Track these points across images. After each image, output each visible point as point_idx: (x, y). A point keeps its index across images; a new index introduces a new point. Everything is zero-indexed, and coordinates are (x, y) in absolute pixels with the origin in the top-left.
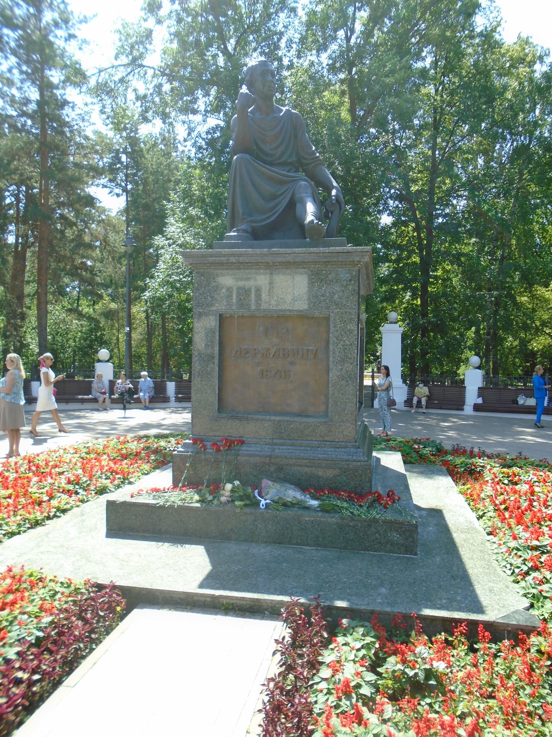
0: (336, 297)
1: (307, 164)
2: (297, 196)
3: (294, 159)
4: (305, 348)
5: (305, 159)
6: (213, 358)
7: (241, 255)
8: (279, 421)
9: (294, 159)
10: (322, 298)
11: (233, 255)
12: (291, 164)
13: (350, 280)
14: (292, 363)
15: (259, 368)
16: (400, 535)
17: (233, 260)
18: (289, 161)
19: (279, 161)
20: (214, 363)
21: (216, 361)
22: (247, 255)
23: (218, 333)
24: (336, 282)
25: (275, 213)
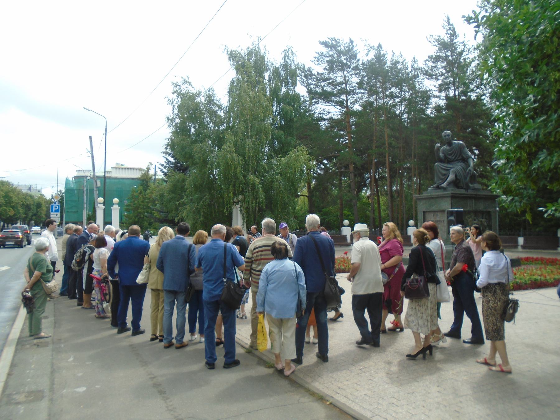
9: (460, 158)
12: (460, 159)
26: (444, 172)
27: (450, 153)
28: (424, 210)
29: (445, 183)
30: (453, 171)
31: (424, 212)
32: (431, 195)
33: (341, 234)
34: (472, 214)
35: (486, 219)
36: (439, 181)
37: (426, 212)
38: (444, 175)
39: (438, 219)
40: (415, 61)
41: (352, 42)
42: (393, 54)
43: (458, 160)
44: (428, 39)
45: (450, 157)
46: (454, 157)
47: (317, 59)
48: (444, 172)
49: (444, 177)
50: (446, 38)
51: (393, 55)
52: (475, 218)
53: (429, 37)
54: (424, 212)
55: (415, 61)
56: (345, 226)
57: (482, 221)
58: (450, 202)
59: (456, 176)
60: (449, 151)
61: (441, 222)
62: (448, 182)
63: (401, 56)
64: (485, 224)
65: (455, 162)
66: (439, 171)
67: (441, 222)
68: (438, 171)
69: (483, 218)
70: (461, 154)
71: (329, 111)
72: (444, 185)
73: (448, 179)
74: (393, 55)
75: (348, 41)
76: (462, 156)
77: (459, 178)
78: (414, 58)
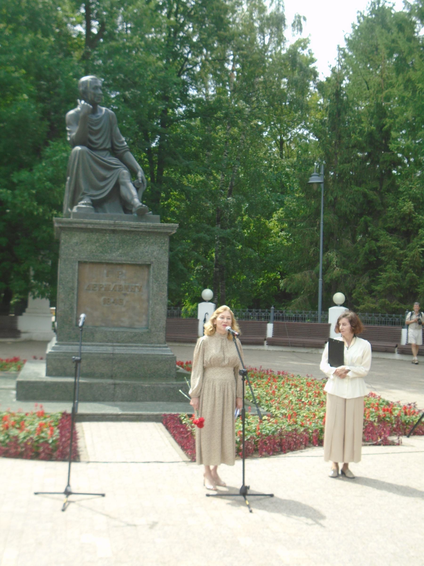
0: (155, 253)
1: (118, 150)
2: (121, 180)
3: (109, 146)
5: (118, 147)
6: (73, 290)
7: (96, 224)
8: (117, 332)
10: (146, 254)
11: (90, 223)
13: (164, 243)
14: (125, 295)
17: (90, 226)
20: (73, 293)
21: (76, 292)
22: (99, 224)
23: (77, 274)
24: (156, 244)
25: (105, 191)
26: (103, 173)
27: (95, 128)
28: (84, 257)
31: (80, 263)
32: (114, 225)
37: (85, 263)
39: (122, 283)
43: (105, 149)
45: (93, 138)
46: (101, 141)
48: (103, 173)
49: (102, 184)
54: (80, 263)
58: (166, 247)
60: (92, 125)
66: (91, 167)
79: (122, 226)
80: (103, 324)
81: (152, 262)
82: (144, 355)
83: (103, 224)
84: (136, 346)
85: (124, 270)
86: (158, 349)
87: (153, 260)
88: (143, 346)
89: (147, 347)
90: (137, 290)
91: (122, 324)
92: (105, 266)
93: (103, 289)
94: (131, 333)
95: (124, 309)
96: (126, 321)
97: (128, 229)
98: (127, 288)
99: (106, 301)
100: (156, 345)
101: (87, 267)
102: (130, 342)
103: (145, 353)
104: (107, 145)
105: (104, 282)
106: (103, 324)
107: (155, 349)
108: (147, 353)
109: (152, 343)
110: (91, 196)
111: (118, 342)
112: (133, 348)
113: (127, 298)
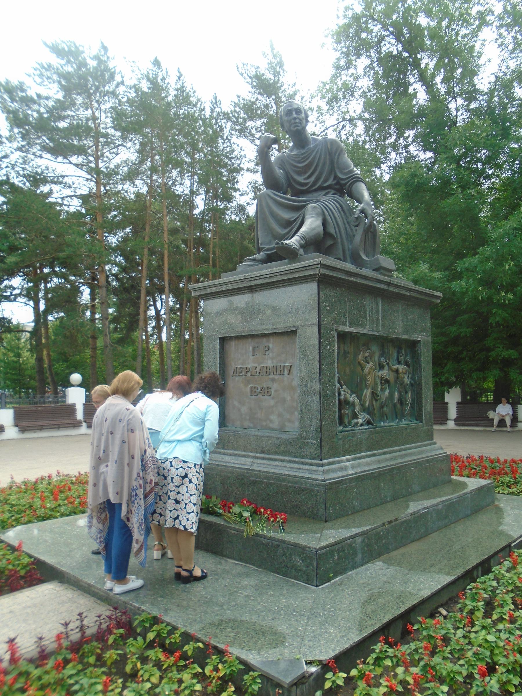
4: (283, 365)
8: (262, 437)
12: (329, 187)
14: (273, 380)
15: (251, 385)
16: (303, 561)
17: (223, 288)
18: (326, 185)
19: (314, 188)
26: (286, 215)
29: (296, 238)
30: (315, 207)
31: (223, 340)
33: (65, 401)
34: (375, 348)
35: (406, 364)
36: (270, 243)
37: (231, 338)
38: (288, 224)
39: (269, 363)
40: (216, 102)
41: (105, 48)
42: (178, 74)
43: (321, 188)
44: (240, 69)
45: (301, 179)
46: (312, 179)
47: (38, 72)
48: (286, 215)
49: (286, 231)
50: (269, 76)
51: (179, 78)
52: (383, 360)
53: (240, 66)
54: (223, 340)
55: (216, 102)
56: (73, 386)
57: (397, 371)
59: (324, 224)
60: (299, 162)
61: (281, 374)
62: (303, 238)
63: (194, 92)
64: (407, 380)
65: (315, 194)
67: (281, 374)
68: (267, 213)
69: (399, 363)
70: (332, 170)
71: (64, 174)
72: (294, 242)
73: (303, 229)
74: (179, 78)
75: (99, 45)
76: (336, 177)
77: (332, 230)
78: (216, 99)
79: (253, 279)
80: (251, 425)
81: (298, 327)
82: (285, 475)
83: (235, 282)
84: (282, 461)
85: (272, 343)
86: (307, 467)
87: (298, 323)
88: (290, 462)
89: (295, 462)
90: (286, 372)
91: (271, 425)
92: (250, 340)
93: (249, 374)
94: (278, 439)
95: (272, 403)
96: (275, 421)
97: (261, 282)
98: (275, 369)
99: (253, 391)
100: (307, 461)
101: (233, 343)
102: (276, 453)
103: (286, 473)
104: (326, 181)
105: (250, 365)
106: (251, 425)
107: (302, 466)
108: (291, 473)
109: (303, 457)
110: (268, 250)
111: (263, 452)
112: (277, 463)
113: (275, 386)
